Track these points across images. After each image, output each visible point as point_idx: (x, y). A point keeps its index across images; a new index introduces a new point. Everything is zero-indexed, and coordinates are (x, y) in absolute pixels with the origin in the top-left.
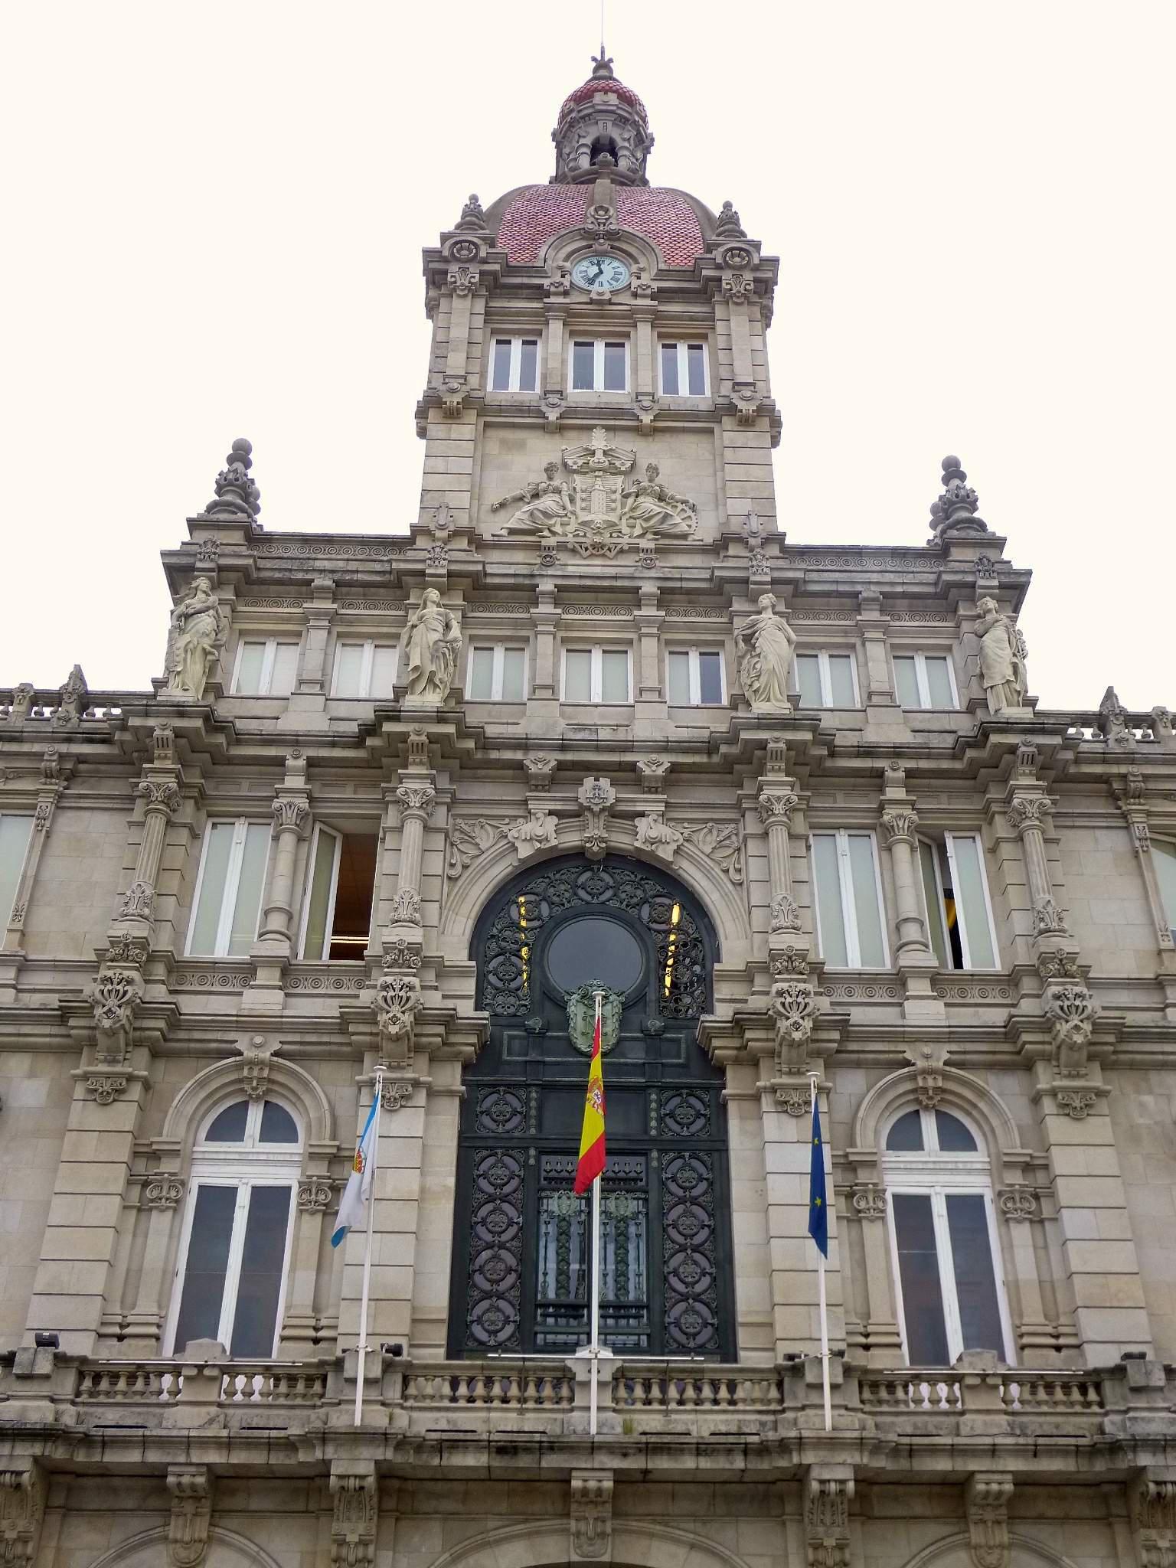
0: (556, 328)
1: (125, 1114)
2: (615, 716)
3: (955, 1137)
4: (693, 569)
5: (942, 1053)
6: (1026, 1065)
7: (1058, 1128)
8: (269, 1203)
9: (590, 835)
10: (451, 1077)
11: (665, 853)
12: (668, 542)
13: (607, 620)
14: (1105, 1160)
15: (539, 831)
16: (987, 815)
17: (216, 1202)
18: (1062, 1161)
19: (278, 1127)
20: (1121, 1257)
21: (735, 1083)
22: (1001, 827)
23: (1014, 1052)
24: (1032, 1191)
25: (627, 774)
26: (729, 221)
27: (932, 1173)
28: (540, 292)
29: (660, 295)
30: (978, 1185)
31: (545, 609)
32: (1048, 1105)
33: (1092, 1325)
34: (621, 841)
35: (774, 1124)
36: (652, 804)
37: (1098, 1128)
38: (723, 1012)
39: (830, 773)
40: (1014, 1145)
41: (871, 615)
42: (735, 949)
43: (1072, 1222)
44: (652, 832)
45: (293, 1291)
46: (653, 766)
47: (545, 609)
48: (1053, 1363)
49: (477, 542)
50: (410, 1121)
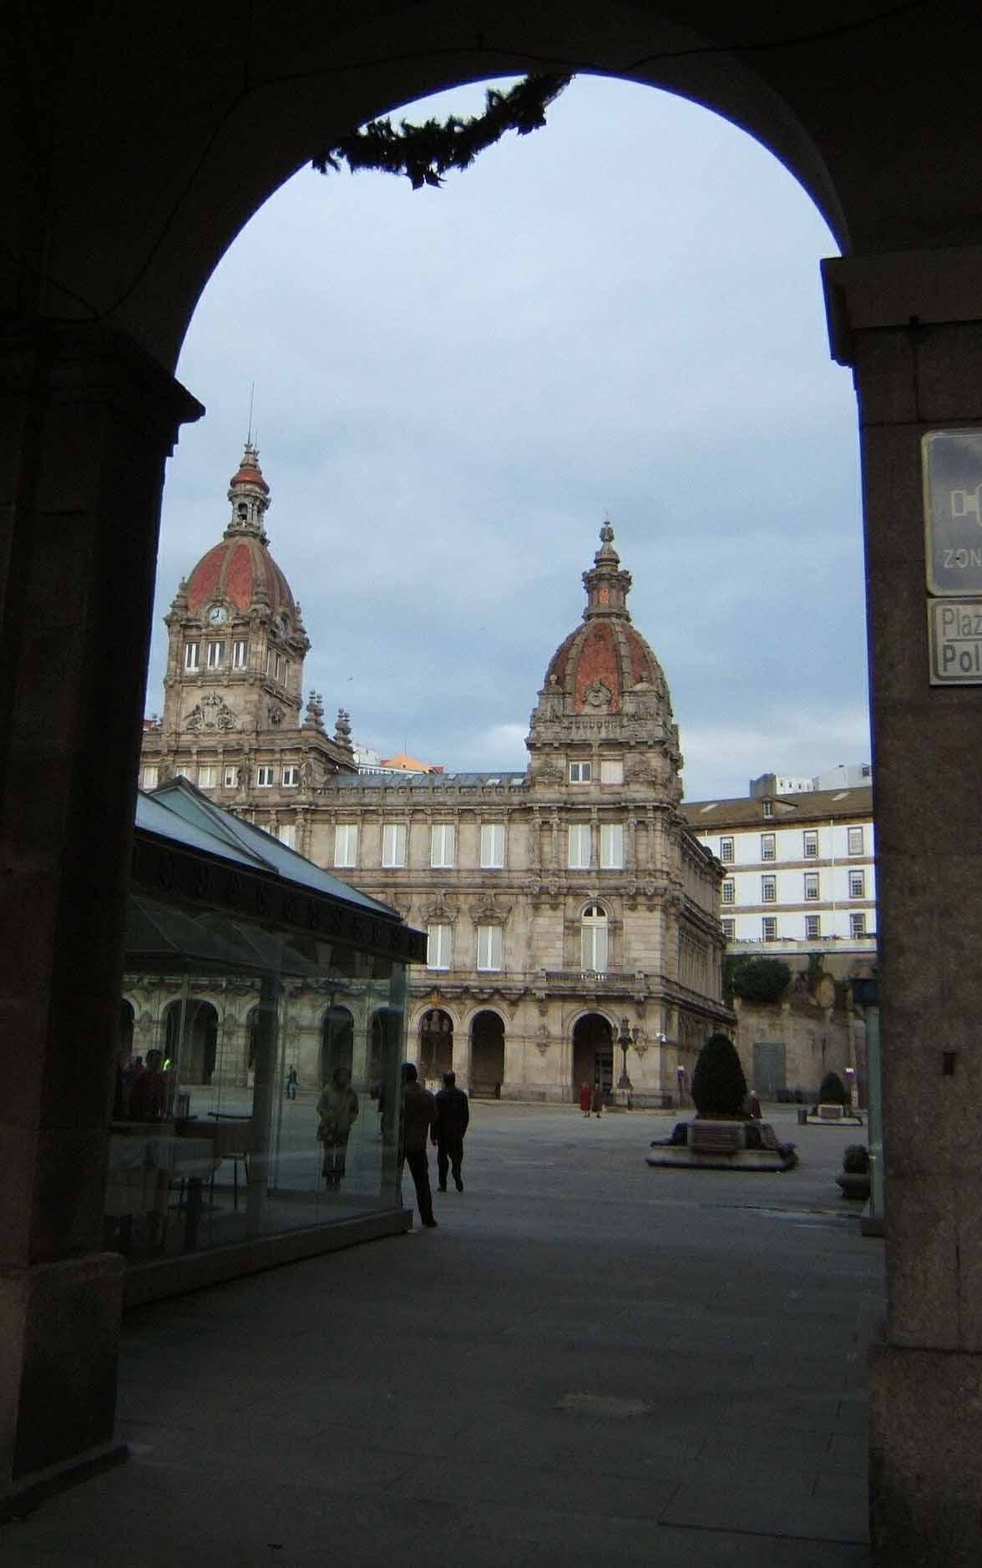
28: (199, 628)
41: (277, 756)
49: (178, 734)
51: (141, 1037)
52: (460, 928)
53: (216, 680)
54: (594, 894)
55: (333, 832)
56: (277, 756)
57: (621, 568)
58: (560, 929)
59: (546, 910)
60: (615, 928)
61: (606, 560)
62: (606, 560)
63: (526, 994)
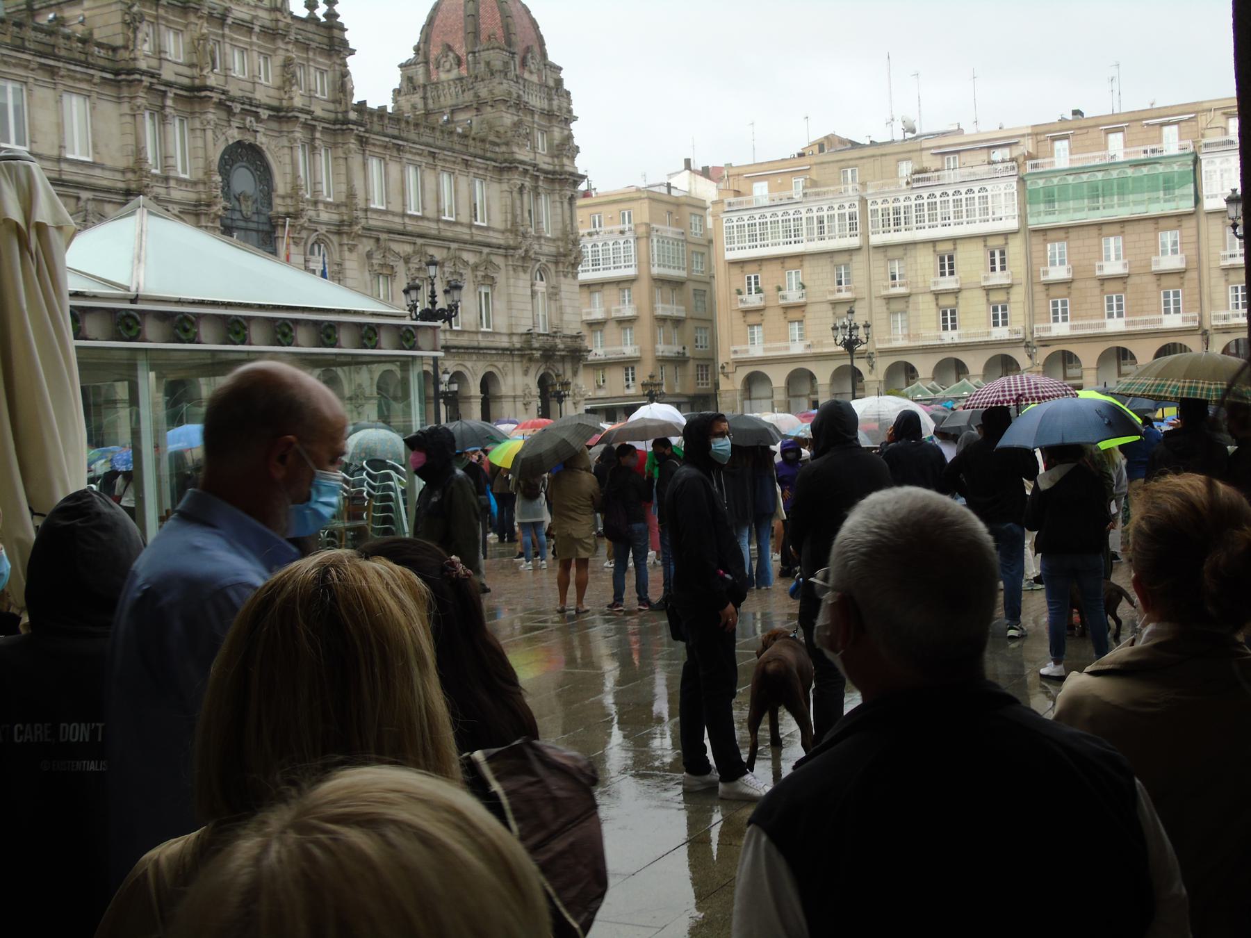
2: (248, 86)
5: (323, 229)
6: (339, 233)
7: (347, 254)
9: (249, 138)
11: (264, 148)
15: (234, 135)
22: (340, 153)
23: (340, 229)
31: (227, 31)
32: (346, 248)
34: (252, 140)
36: (260, 127)
37: (354, 256)
42: (281, 185)
44: (261, 140)
46: (264, 114)
54: (543, 259)
56: (311, 54)
58: (529, 293)
59: (522, 275)
63: (507, 353)
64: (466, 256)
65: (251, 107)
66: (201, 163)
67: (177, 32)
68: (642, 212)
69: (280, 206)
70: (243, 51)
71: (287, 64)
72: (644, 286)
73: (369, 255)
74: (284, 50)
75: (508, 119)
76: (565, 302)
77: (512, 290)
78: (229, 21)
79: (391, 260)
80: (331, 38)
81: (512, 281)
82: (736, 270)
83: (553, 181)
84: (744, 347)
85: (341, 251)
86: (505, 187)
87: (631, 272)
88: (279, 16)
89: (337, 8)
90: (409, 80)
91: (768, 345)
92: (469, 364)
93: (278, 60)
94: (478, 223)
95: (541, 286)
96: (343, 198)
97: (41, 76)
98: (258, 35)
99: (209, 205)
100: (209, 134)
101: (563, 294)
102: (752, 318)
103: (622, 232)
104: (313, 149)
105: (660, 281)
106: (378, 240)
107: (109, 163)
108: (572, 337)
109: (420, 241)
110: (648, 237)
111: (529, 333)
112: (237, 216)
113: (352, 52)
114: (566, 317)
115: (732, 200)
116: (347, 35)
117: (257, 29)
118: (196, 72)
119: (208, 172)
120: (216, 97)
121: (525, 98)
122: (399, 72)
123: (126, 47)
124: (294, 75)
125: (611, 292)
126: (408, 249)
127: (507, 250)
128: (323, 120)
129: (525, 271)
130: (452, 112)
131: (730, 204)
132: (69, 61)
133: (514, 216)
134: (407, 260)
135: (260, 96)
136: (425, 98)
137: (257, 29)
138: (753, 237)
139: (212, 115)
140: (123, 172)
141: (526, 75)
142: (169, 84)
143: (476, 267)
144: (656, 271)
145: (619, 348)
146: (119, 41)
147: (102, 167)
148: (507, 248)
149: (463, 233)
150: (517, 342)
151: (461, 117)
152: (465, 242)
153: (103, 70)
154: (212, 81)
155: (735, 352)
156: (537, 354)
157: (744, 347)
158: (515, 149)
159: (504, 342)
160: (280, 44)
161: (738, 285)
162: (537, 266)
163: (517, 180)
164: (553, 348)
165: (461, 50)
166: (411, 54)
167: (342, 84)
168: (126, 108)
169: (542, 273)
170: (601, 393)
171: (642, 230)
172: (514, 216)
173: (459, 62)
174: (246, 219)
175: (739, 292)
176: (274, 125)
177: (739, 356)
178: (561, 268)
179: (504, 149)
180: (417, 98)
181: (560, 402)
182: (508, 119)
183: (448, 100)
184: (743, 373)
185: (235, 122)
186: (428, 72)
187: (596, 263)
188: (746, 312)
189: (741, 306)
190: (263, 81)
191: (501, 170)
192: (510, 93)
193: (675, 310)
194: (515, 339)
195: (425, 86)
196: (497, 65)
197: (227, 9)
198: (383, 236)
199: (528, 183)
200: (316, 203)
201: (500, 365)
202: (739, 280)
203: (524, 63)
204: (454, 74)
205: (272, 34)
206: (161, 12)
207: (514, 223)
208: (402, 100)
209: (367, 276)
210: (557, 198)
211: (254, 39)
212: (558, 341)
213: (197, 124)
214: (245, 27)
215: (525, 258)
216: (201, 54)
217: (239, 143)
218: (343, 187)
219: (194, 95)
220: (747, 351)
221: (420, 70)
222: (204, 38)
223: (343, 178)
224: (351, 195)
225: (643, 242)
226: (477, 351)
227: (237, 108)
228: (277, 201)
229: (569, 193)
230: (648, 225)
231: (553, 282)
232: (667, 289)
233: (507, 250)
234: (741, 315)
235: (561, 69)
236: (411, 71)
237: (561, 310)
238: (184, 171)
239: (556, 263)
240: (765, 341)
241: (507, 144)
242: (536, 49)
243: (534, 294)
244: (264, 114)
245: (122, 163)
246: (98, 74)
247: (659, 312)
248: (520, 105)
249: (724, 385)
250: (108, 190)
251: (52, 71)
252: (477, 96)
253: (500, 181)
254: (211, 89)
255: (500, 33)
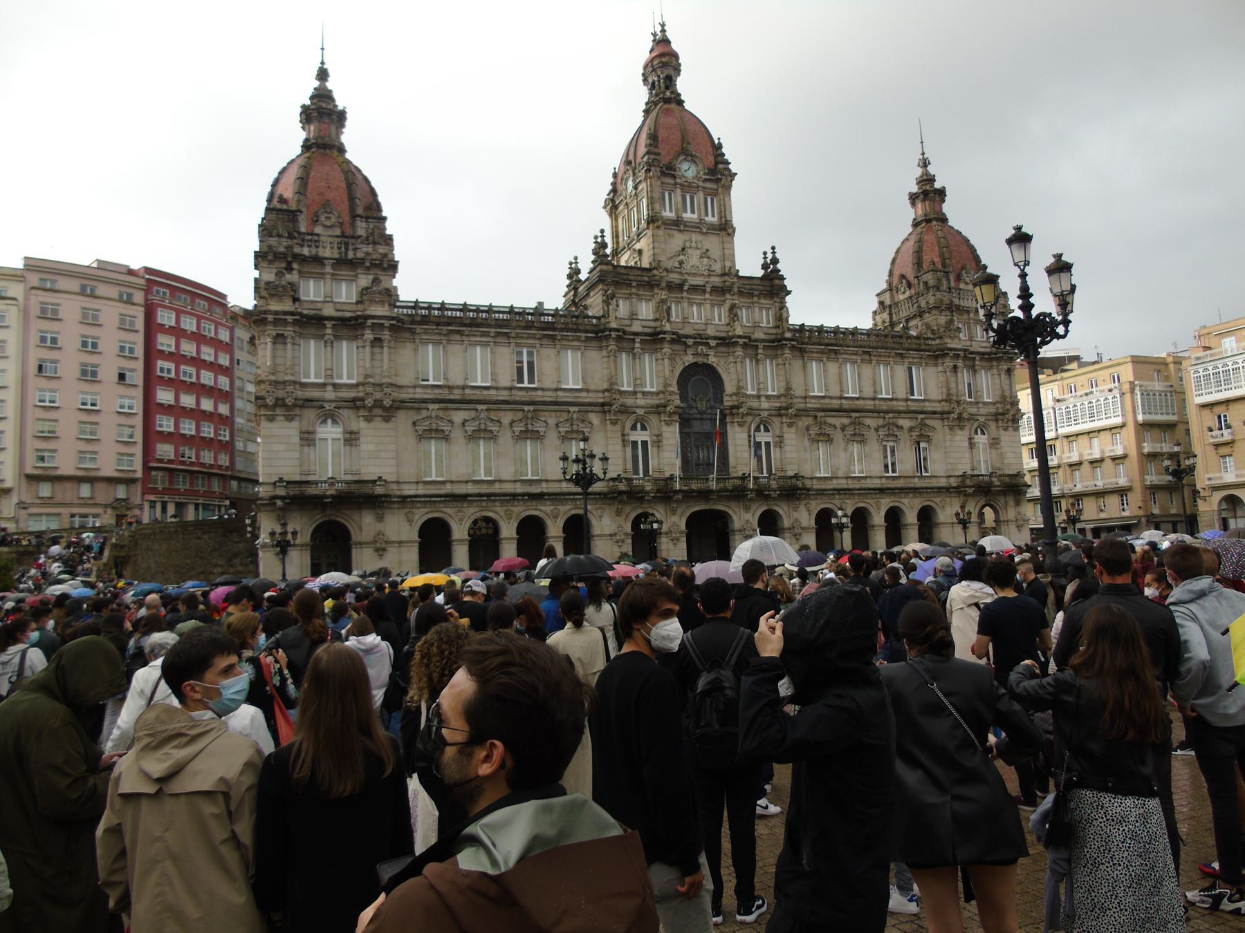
0: (679, 191)
1: (618, 427)
2: (703, 327)
3: (767, 430)
4: (716, 281)
5: (765, 414)
6: (781, 416)
7: (786, 429)
8: (645, 443)
9: (701, 360)
10: (676, 418)
12: (711, 273)
13: (698, 297)
14: (794, 436)
15: (689, 359)
16: (776, 356)
17: (635, 444)
18: (786, 436)
19: (644, 428)
20: (794, 455)
21: (728, 419)
22: (780, 361)
23: (780, 412)
24: (780, 442)
25: (707, 344)
26: (720, 146)
27: (763, 437)
29: (706, 180)
30: (769, 439)
31: (685, 294)
33: (788, 467)
35: (737, 428)
36: (711, 352)
37: (793, 429)
38: (726, 404)
39: (750, 344)
40: (778, 433)
41: (755, 299)
42: (729, 387)
43: (787, 448)
44: (712, 360)
45: (652, 463)
46: (713, 343)
47: (685, 294)
48: (782, 474)
50: (671, 429)
51: (671, 546)
52: (902, 444)
53: (698, 227)
54: (982, 419)
55: (804, 367)
56: (755, 299)
57: (937, 185)
58: (966, 444)
59: (959, 432)
60: (995, 443)
61: (927, 180)
62: (927, 180)
63: (947, 490)
64: (901, 422)
65: (701, 339)
66: (661, 380)
67: (648, 301)
68: (1127, 373)
69: (728, 401)
70: (699, 305)
71: (732, 307)
72: (1130, 431)
73: (807, 429)
74: (730, 300)
75: (943, 320)
76: (1005, 449)
77: (948, 444)
78: (686, 288)
79: (828, 430)
80: (772, 286)
81: (948, 437)
82: (1206, 412)
83: (991, 360)
84: (1218, 475)
85: (781, 431)
86: (940, 368)
87: (1118, 421)
88: (726, 278)
89: (779, 266)
90: (881, 303)
91: (1238, 472)
92: (906, 501)
93: (727, 306)
94: (916, 397)
95: (981, 439)
96: (782, 391)
97: (545, 342)
98: (711, 293)
99: (665, 406)
100: (666, 361)
101: (1003, 444)
102: (1223, 451)
103: (1110, 390)
104: (757, 361)
105: (1147, 426)
106: (816, 417)
107: (592, 387)
108: (1010, 476)
109: (854, 415)
110: (1132, 391)
111: (964, 475)
112: (695, 411)
113: (789, 293)
114: (1006, 461)
115: (1201, 354)
116: (786, 282)
117: (708, 289)
118: (658, 324)
119: (666, 385)
120: (668, 337)
121: (956, 301)
122: (876, 300)
123: (603, 316)
124: (736, 315)
125: (1106, 436)
126: (846, 421)
127: (943, 415)
128: (763, 341)
129: (962, 428)
130: (907, 321)
131: (1198, 358)
132: (562, 330)
133: (949, 390)
134: (843, 429)
135: (711, 332)
136: (890, 314)
137: (708, 289)
138: (1219, 384)
139: (667, 349)
140: (603, 391)
141: (962, 286)
142: (637, 334)
143: (911, 429)
144: (1140, 418)
145: (1113, 480)
146: (601, 313)
147: (588, 391)
148: (942, 413)
149: (901, 406)
150: (954, 482)
151: (912, 323)
152: (899, 412)
153: (587, 332)
154: (668, 328)
155: (1210, 479)
156: (971, 491)
157: (1218, 475)
158: (949, 341)
159: (943, 482)
160: (728, 296)
161: (1210, 424)
162: (976, 424)
163: (949, 363)
164: (990, 484)
165: (911, 276)
166: (884, 286)
167: (781, 316)
168: (605, 353)
169: (982, 429)
170: (1103, 516)
171: (1126, 387)
172: (949, 390)
173: (909, 285)
174: (701, 413)
175: (1211, 430)
176: (723, 349)
177: (1213, 482)
178: (1000, 423)
179: (938, 341)
180: (885, 316)
181: (841, 532)
182: (943, 320)
183: (904, 313)
184: (1219, 495)
185: (690, 352)
186: (892, 297)
187: (1092, 416)
188: (1217, 446)
189: (1212, 440)
190: (717, 321)
191: (937, 357)
192: (942, 301)
193: (1166, 448)
194: (952, 480)
195: (890, 306)
196: (931, 283)
197: (685, 281)
198: (819, 414)
199: (960, 363)
200: (759, 397)
201: (938, 500)
202: (1210, 419)
203: (958, 278)
204: (908, 294)
205: (720, 291)
206: (634, 290)
207: (949, 394)
208: (878, 317)
209: (807, 443)
210: (995, 371)
211: (708, 296)
212: (994, 479)
213: (659, 356)
214: (695, 289)
215: (960, 418)
216: (664, 311)
217: (694, 365)
218: (783, 384)
219: (654, 339)
220: (1221, 478)
221: (887, 295)
222: (663, 301)
223: (782, 378)
224: (788, 389)
225: (1128, 397)
226: (915, 491)
227: (690, 342)
228: (726, 398)
229: (1006, 367)
230: (1131, 382)
231: (994, 434)
232: (1156, 432)
233: (943, 415)
234: (1212, 448)
235: (998, 277)
236: (882, 299)
237: (1002, 456)
238: (652, 386)
239: (997, 421)
240: (1236, 469)
241: (941, 338)
242: (971, 265)
243: (972, 445)
244: (713, 343)
245: (605, 386)
246: (583, 335)
247: (1146, 451)
248: (952, 308)
249: (1202, 506)
250: (590, 404)
251: (553, 338)
252: (919, 307)
253: (936, 365)
254: (664, 333)
255: (937, 260)
